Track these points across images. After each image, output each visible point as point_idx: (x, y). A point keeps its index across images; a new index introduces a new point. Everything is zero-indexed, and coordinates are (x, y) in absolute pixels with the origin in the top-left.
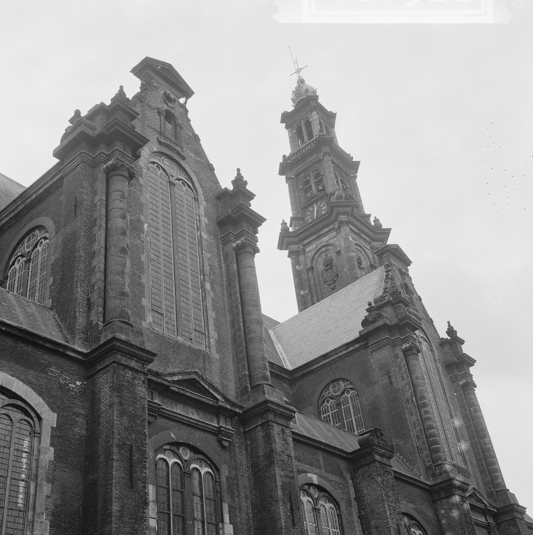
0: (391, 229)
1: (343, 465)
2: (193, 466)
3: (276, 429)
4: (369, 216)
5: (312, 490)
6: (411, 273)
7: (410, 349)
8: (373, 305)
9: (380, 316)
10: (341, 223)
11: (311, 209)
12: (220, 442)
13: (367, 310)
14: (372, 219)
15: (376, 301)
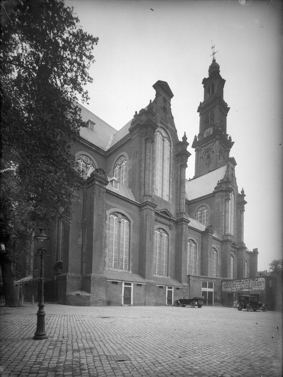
0: (234, 142)
1: (200, 235)
2: (163, 234)
3: (184, 226)
4: (228, 135)
5: (190, 241)
6: (235, 169)
7: (227, 199)
8: (220, 182)
9: (221, 187)
10: (217, 139)
11: (207, 131)
12: (170, 228)
13: (217, 184)
14: (229, 137)
15: (221, 180)
